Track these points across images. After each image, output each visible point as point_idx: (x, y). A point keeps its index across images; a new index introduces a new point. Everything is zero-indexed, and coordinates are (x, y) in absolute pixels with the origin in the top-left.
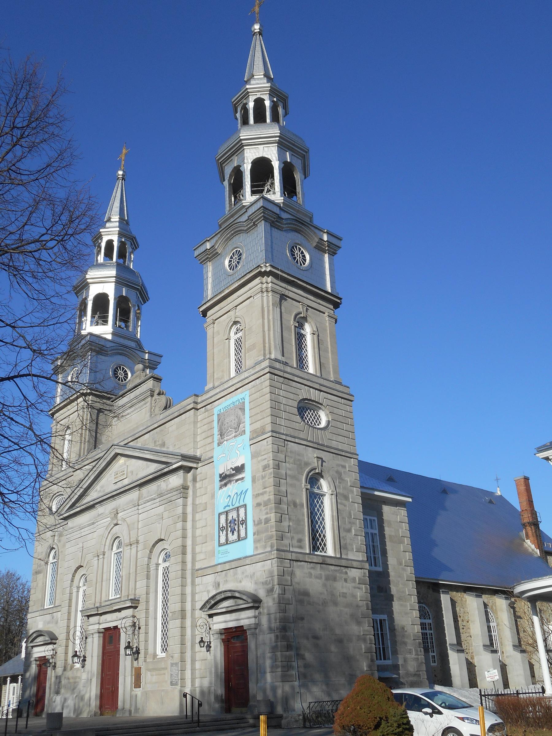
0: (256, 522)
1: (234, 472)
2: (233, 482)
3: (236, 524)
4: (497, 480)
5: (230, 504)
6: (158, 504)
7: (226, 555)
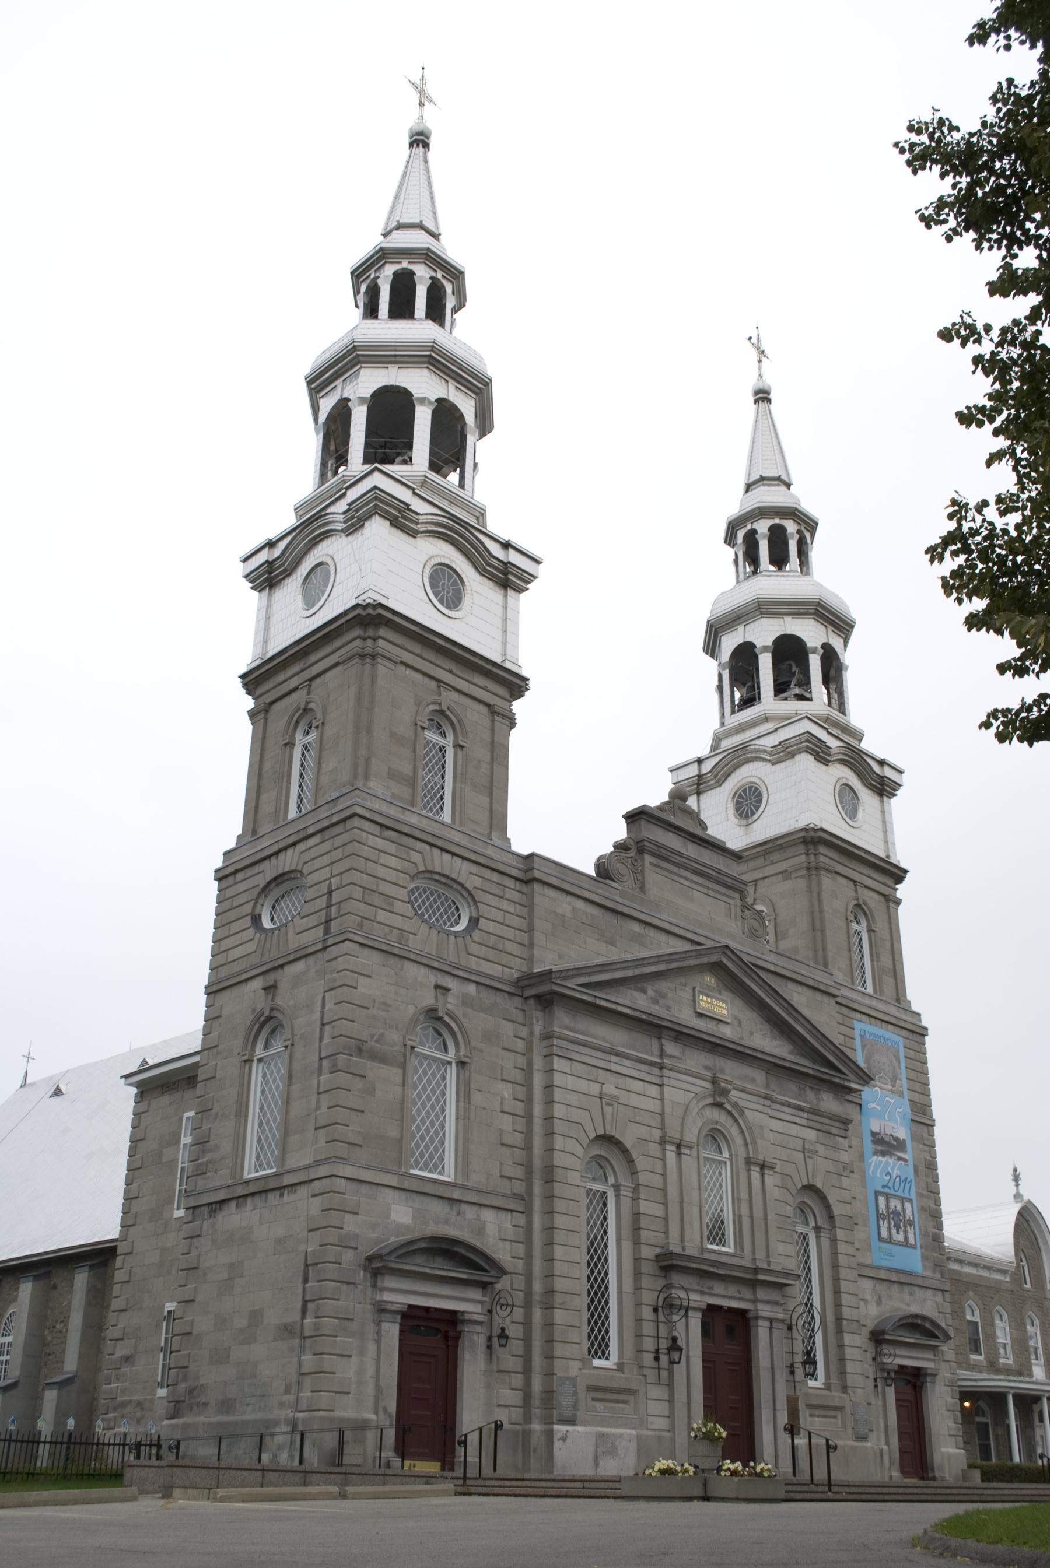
1: (895, 1143)
3: (901, 1220)
4: (28, 1057)
6: (804, 1122)
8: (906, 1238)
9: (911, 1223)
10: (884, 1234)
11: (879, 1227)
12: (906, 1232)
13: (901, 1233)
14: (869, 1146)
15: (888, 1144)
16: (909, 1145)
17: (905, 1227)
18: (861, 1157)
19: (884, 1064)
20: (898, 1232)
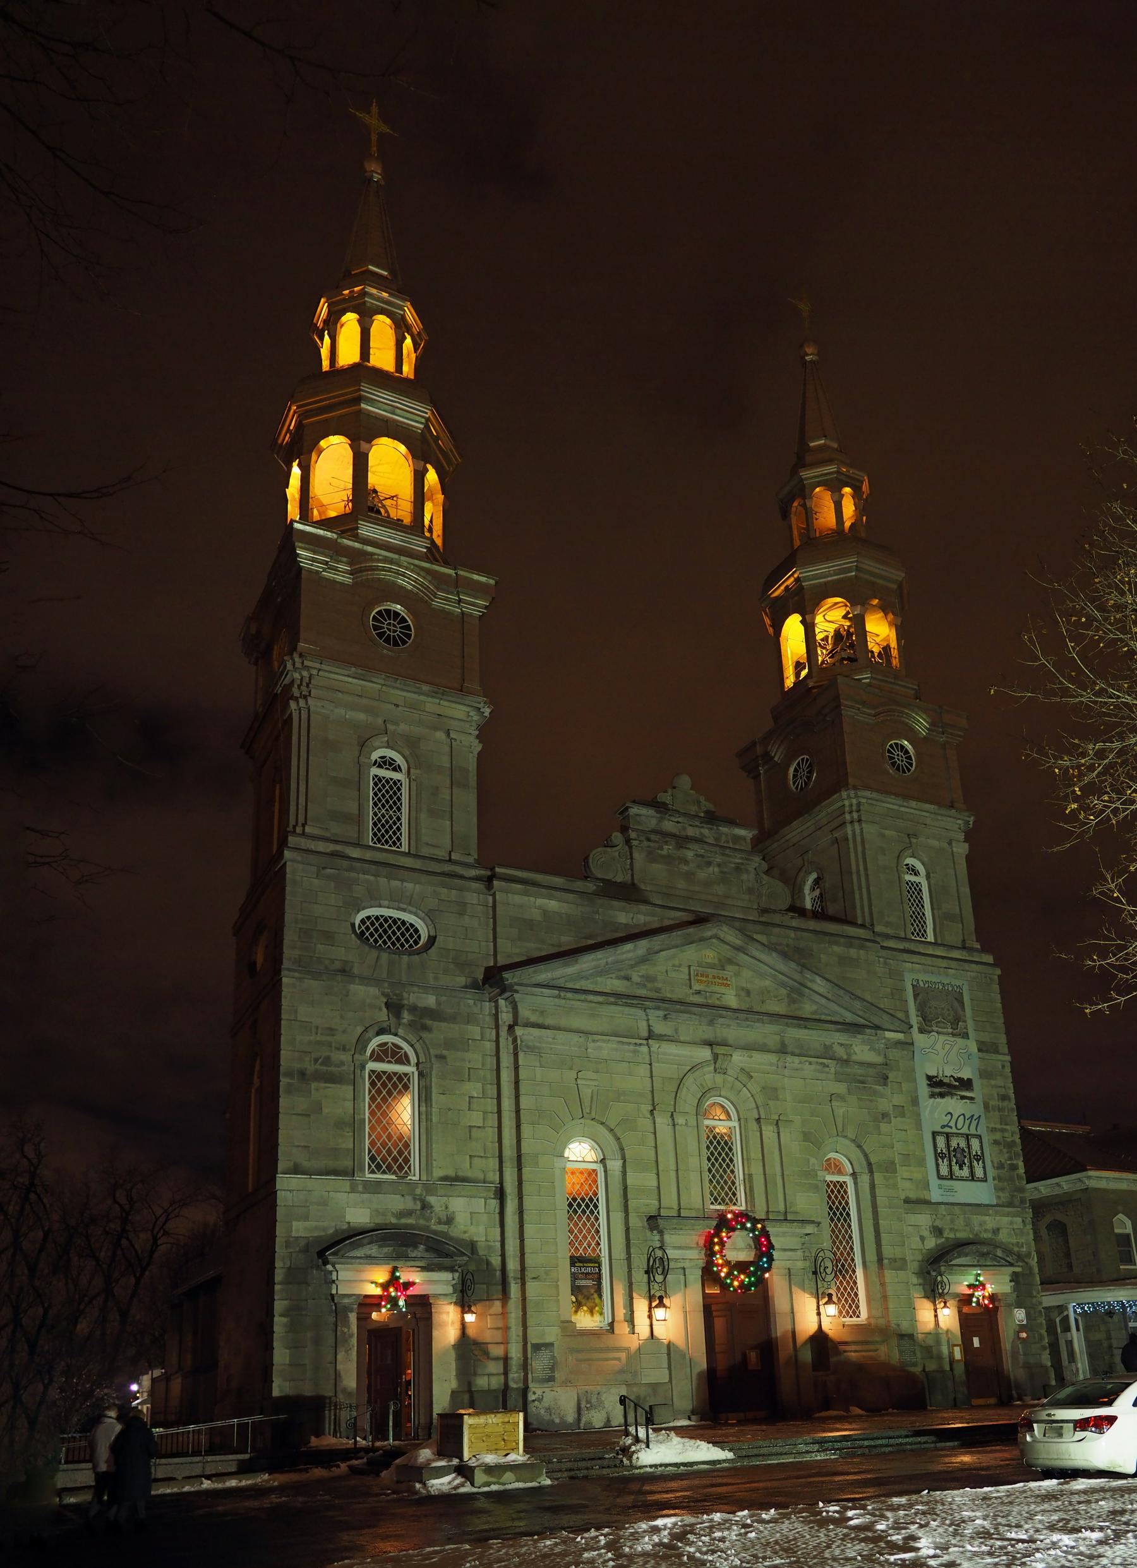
0: (996, 1165)
1: (957, 1084)
2: (955, 1097)
3: (965, 1157)
5: (952, 1124)
7: (952, 1194)
8: (972, 1173)
9: (979, 1158)
10: (944, 1171)
11: (937, 1165)
12: (971, 1167)
13: (966, 1168)
14: (923, 1089)
15: (949, 1086)
16: (976, 1084)
17: (971, 1163)
18: (915, 1102)
19: (943, 1009)
20: (961, 1168)
